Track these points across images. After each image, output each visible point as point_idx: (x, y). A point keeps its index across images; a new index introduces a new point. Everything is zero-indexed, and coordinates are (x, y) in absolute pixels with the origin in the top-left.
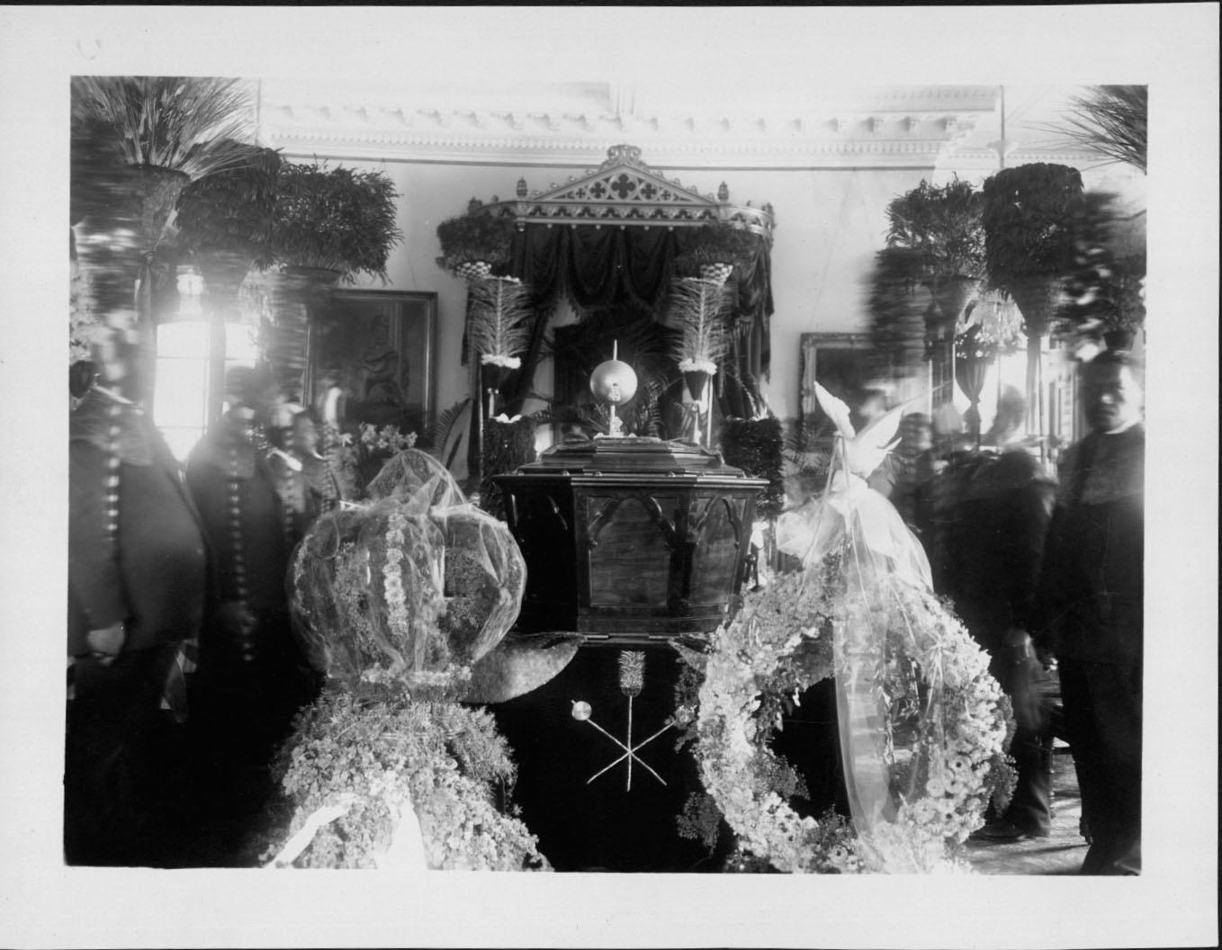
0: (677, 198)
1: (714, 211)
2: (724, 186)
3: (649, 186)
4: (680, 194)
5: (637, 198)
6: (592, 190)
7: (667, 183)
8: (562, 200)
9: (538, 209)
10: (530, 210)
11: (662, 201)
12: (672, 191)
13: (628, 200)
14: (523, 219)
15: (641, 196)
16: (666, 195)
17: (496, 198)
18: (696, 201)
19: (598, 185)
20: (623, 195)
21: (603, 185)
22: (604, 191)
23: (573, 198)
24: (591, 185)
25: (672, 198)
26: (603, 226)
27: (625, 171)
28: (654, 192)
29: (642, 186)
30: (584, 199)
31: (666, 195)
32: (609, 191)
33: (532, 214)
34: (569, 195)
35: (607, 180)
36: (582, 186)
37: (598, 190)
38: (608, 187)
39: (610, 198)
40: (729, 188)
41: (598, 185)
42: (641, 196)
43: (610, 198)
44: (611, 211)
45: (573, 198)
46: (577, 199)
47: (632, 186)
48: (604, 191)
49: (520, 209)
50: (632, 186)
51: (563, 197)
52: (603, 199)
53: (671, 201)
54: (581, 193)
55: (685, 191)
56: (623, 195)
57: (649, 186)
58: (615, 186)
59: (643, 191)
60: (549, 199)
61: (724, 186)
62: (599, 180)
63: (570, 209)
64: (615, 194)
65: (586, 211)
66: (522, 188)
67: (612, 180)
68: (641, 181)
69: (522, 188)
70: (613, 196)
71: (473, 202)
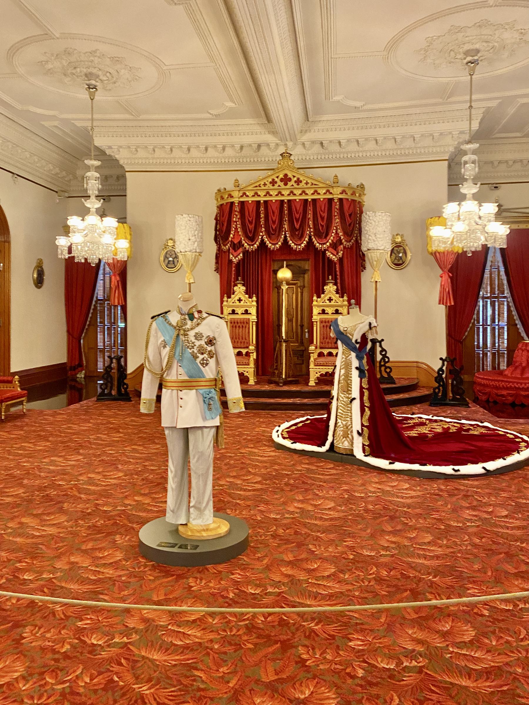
0: (312, 184)
3: (298, 179)
6: (271, 183)
9: (245, 194)
11: (305, 186)
13: (287, 187)
15: (294, 184)
16: (307, 183)
18: (321, 185)
19: (273, 180)
20: (286, 184)
21: (276, 179)
22: (276, 182)
24: (270, 180)
27: (286, 172)
28: (301, 182)
29: (295, 179)
30: (266, 187)
31: (307, 183)
32: (279, 183)
34: (259, 186)
35: (277, 177)
37: (273, 183)
41: (273, 180)
43: (279, 186)
44: (280, 193)
46: (263, 187)
47: (290, 180)
48: (276, 182)
49: (236, 194)
50: (290, 180)
52: (276, 186)
53: (309, 186)
54: (265, 185)
56: (286, 184)
57: (298, 179)
58: (282, 180)
59: (295, 182)
62: (274, 177)
63: (259, 193)
64: (282, 184)
66: (237, 184)
67: (280, 178)
68: (294, 177)
69: (237, 184)
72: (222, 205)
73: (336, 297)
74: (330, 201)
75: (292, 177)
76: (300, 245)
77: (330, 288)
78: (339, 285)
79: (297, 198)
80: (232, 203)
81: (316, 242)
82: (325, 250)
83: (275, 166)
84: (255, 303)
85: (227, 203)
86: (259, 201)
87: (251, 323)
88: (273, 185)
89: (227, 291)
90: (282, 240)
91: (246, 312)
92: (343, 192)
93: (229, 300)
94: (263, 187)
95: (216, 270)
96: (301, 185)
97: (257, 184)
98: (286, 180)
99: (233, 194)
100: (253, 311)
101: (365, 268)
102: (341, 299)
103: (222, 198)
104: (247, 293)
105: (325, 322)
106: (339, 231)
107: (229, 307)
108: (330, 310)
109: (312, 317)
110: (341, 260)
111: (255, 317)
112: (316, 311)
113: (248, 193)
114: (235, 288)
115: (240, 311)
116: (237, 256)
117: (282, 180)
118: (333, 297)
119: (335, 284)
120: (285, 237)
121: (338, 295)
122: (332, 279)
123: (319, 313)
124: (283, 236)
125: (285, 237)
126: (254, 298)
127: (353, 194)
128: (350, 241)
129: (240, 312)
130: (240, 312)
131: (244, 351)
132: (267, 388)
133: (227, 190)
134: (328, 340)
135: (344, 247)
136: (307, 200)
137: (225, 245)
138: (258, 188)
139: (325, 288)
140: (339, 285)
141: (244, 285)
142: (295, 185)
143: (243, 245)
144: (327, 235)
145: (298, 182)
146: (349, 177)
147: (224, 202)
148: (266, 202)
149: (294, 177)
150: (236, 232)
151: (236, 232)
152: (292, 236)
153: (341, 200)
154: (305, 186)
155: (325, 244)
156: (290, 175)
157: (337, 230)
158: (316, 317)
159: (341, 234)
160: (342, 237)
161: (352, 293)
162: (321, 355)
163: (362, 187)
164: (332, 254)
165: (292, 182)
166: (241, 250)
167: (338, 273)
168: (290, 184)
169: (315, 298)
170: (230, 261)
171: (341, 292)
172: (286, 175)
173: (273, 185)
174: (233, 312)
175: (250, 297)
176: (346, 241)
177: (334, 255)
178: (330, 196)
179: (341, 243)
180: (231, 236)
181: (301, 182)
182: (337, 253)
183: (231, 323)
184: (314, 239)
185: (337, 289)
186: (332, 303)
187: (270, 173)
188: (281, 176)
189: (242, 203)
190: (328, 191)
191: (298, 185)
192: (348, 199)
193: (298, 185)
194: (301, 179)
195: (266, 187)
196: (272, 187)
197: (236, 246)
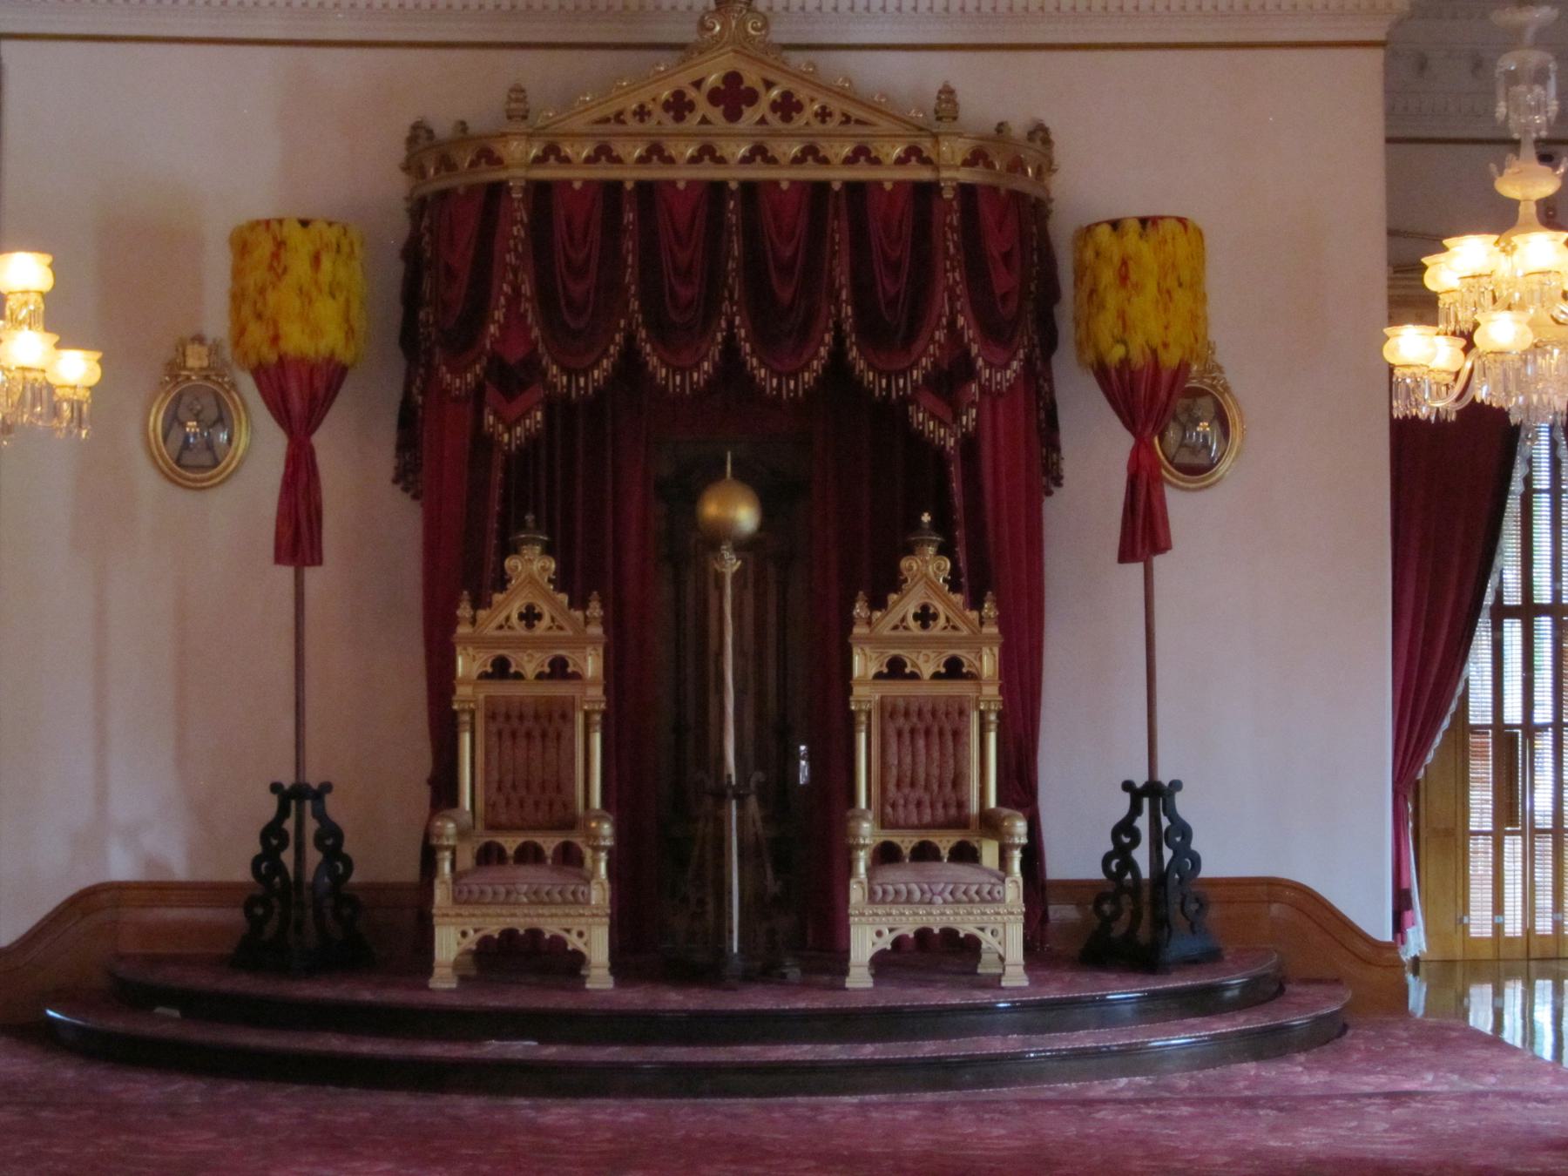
0: (847, 119)
1: (926, 145)
2: (947, 93)
4: (856, 112)
5: (763, 121)
6: (667, 106)
7: (828, 90)
8: (601, 128)
10: (534, 152)
12: (836, 106)
14: (520, 172)
15: (770, 117)
17: (463, 125)
21: (692, 94)
22: (691, 106)
23: (623, 122)
25: (838, 118)
26: (691, 184)
28: (799, 107)
29: (775, 93)
31: (824, 115)
32: (703, 107)
33: (540, 160)
34: (619, 117)
35: (697, 84)
36: (644, 96)
37: (679, 106)
38: (699, 97)
39: (704, 121)
40: (961, 98)
41: (679, 95)
42: (770, 117)
43: (704, 121)
45: (623, 122)
47: (752, 97)
48: (691, 106)
51: (606, 120)
52: (692, 120)
53: (833, 124)
54: (642, 113)
55: (861, 103)
56: (733, 115)
57: (787, 95)
58: (715, 97)
59: (775, 106)
60: (579, 124)
61: (947, 93)
62: (683, 80)
63: (619, 148)
64: (716, 114)
65: (656, 152)
66: (518, 106)
70: (710, 116)
71: (419, 134)
72: (444, 195)
73: (949, 606)
74: (925, 192)
75: (760, 88)
76: (795, 375)
77: (927, 567)
78: (961, 551)
79: (785, 175)
80: (497, 190)
81: (862, 364)
82: (905, 401)
83: (686, 32)
84: (596, 630)
85: (471, 189)
86: (617, 185)
87: (580, 719)
88: (679, 118)
89: (458, 573)
90: (715, 352)
91: (559, 670)
92: (977, 158)
93: (482, 614)
94: (633, 124)
95: (406, 475)
96: (800, 120)
97: (609, 110)
98: (733, 96)
99: (499, 149)
100: (592, 665)
101: (1058, 480)
102: (974, 615)
103: (446, 164)
104: (563, 581)
105: (907, 714)
106: (961, 321)
107: (480, 643)
108: (927, 664)
109: (848, 691)
110: (969, 445)
111: (596, 692)
112: (863, 664)
113: (567, 150)
114: (510, 563)
115: (530, 664)
116: (518, 422)
117: (715, 97)
118: (939, 607)
119: (944, 550)
120: (731, 339)
121: (958, 598)
122: (937, 525)
123: (879, 676)
124: (719, 337)
125: (731, 339)
126: (595, 609)
127: (1017, 166)
128: (1007, 366)
129: (530, 670)
130: (530, 670)
131: (549, 843)
132: (637, 998)
133: (470, 132)
134: (920, 793)
135: (983, 390)
136: (822, 187)
137: (458, 371)
138: (613, 127)
139: (905, 563)
140: (961, 551)
141: (548, 550)
142: (775, 120)
143: (544, 373)
144: (911, 336)
145: (787, 107)
146: (995, 95)
147: (458, 182)
148: (645, 188)
149: (769, 85)
150: (511, 315)
151: (511, 315)
152: (765, 341)
153: (967, 192)
154: (817, 126)
155: (903, 373)
156: (752, 78)
157: (952, 312)
158: (866, 693)
159: (970, 334)
160: (975, 349)
161: (1006, 580)
162: (886, 855)
163: (1040, 134)
164: (933, 416)
165: (763, 108)
166: (537, 393)
167: (958, 501)
168: (750, 115)
169: (860, 610)
170: (482, 443)
171: (972, 583)
172: (733, 79)
173: (679, 118)
174: (501, 669)
175: (579, 602)
176: (989, 365)
177: (941, 423)
178: (925, 174)
179: (971, 373)
180: (492, 329)
181: (799, 107)
182: (956, 417)
183: (491, 716)
184: (854, 353)
185: (955, 571)
186: (937, 628)
187: (664, 61)
188: (713, 79)
189: (541, 192)
190: (913, 153)
191: (787, 118)
192: (994, 189)
193: (787, 118)
194: (802, 94)
195: (650, 124)
196: (669, 124)
197: (510, 379)
